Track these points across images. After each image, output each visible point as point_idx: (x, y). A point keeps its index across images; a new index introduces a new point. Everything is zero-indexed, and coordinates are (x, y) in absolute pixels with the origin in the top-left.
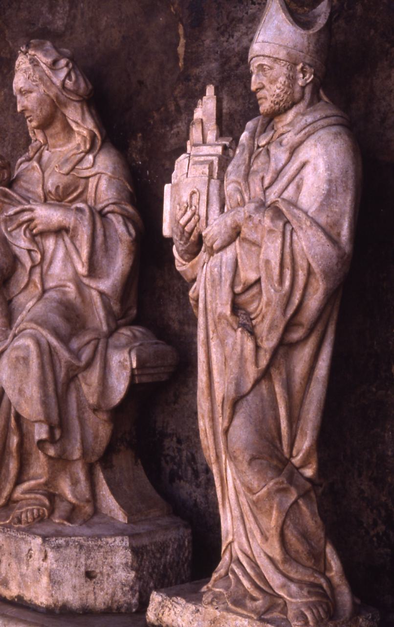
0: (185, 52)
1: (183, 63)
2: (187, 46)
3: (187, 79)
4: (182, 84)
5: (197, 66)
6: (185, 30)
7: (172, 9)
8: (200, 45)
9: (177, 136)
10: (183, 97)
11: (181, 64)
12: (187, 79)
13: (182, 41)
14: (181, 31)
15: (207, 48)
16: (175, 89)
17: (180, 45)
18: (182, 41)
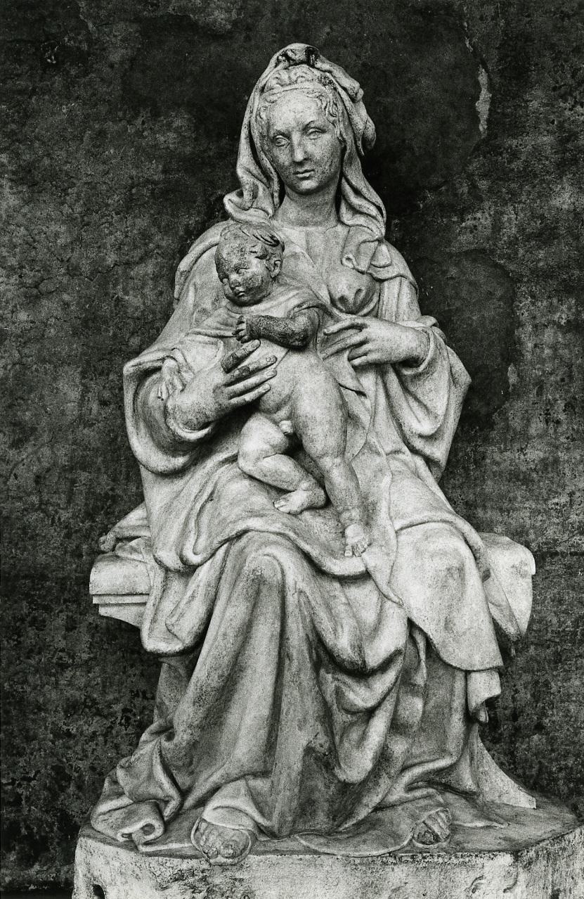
0: (490, 110)
1: (486, 127)
2: (493, 102)
3: (497, 150)
4: (485, 157)
5: (514, 136)
6: (490, 79)
7: (467, 43)
8: (520, 106)
9: (471, 232)
10: (484, 176)
11: (482, 127)
12: (497, 150)
13: (485, 94)
14: (483, 79)
15: (533, 113)
16: (470, 162)
17: (481, 98)
18: (485, 94)
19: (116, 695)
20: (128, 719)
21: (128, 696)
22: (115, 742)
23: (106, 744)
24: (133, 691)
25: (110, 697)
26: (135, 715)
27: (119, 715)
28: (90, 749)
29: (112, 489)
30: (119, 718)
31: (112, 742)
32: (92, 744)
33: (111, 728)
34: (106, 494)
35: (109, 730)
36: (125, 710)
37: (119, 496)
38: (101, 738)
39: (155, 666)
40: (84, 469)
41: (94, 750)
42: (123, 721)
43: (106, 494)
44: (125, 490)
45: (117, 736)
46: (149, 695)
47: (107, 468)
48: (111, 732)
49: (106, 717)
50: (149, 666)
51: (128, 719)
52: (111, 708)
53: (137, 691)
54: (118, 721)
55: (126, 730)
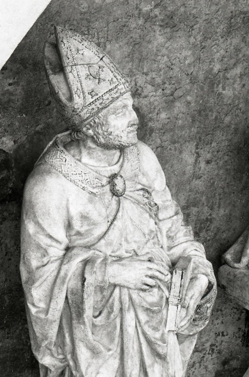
19: (207, 338)
20: (213, 350)
21: (214, 336)
22: (205, 364)
23: (200, 368)
24: (216, 333)
25: (204, 340)
26: (217, 347)
27: (208, 349)
28: (191, 373)
29: (210, 215)
30: (208, 350)
31: (204, 365)
32: (193, 369)
33: (203, 357)
34: (207, 219)
35: (203, 358)
36: (212, 345)
37: (214, 218)
38: (197, 365)
39: (229, 316)
40: (194, 206)
41: (194, 372)
42: (210, 352)
43: (207, 219)
44: (217, 214)
45: (206, 361)
46: (225, 334)
47: (208, 202)
48: (203, 359)
49: (200, 352)
50: (226, 317)
51: (213, 350)
52: (204, 345)
53: (219, 333)
54: (207, 352)
55: (212, 356)
